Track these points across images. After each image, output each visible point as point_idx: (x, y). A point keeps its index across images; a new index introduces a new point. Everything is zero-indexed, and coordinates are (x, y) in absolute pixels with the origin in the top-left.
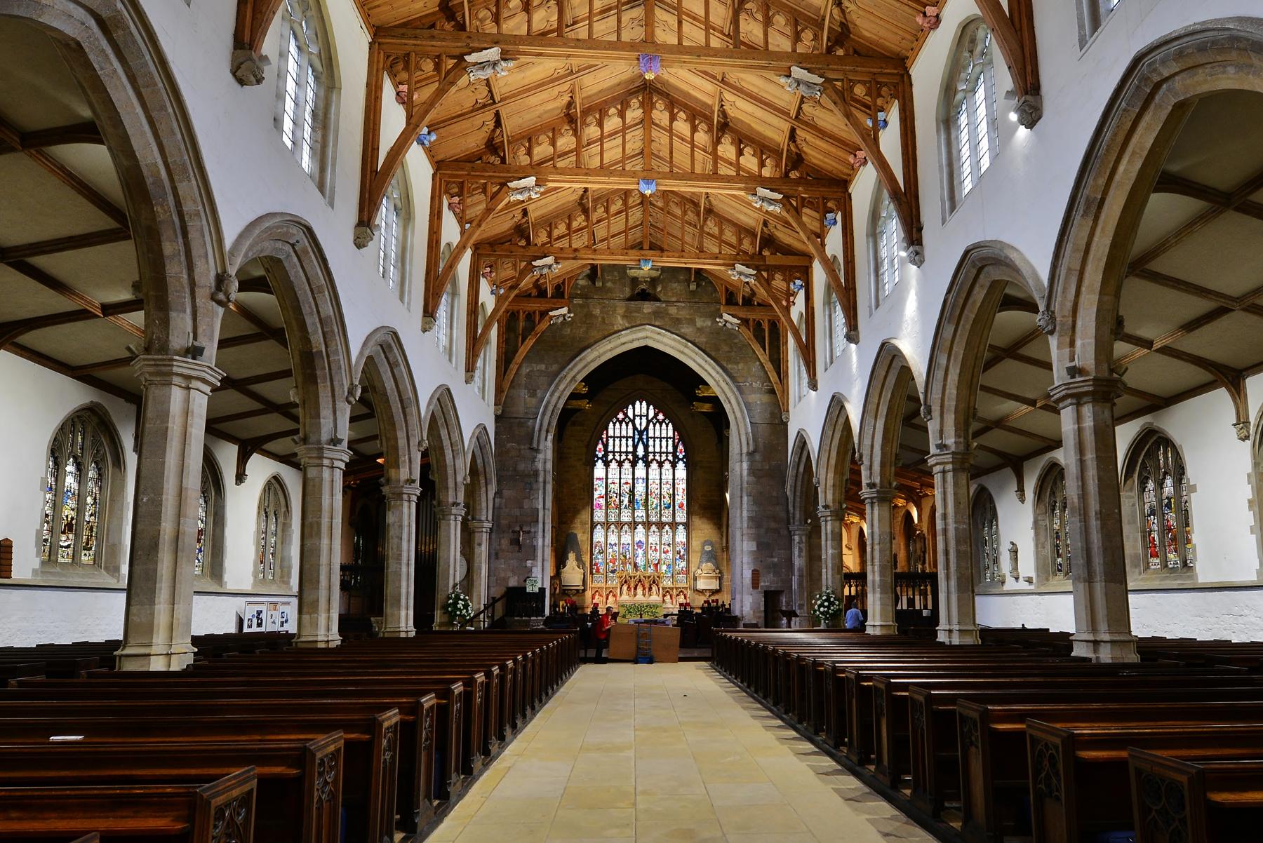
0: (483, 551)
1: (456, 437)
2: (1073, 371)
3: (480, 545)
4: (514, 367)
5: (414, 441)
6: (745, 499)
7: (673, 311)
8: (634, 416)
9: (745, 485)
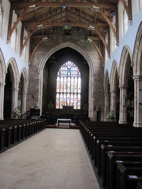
0: (25, 99)
1: (16, 70)
3: (24, 97)
4: (33, 52)
5: (4, 71)
6: (92, 87)
7: (75, 38)
8: (68, 65)
9: (93, 83)
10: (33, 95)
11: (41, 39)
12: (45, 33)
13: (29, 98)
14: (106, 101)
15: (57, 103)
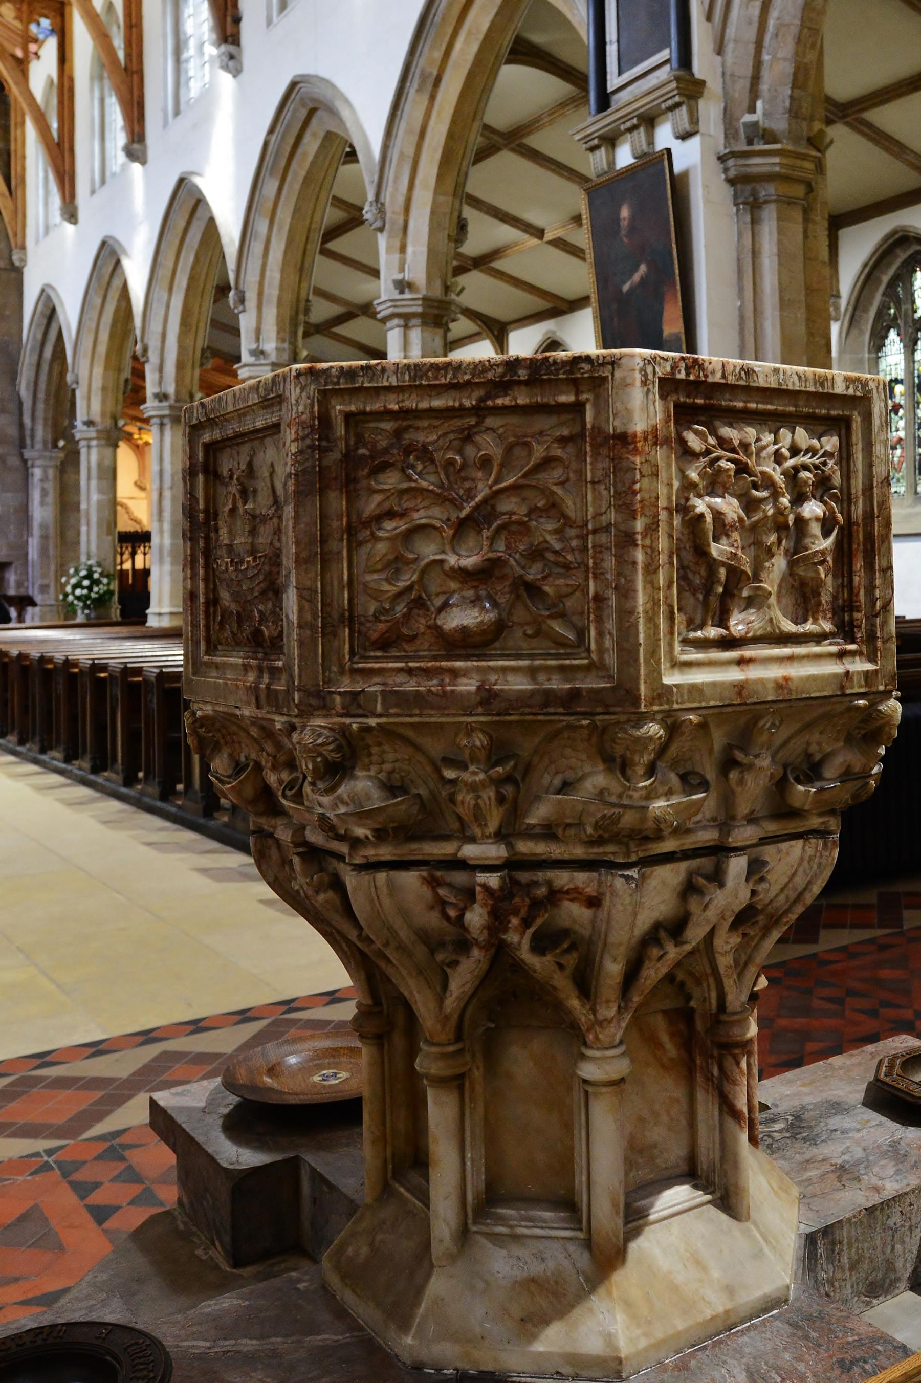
2: (402, 286)
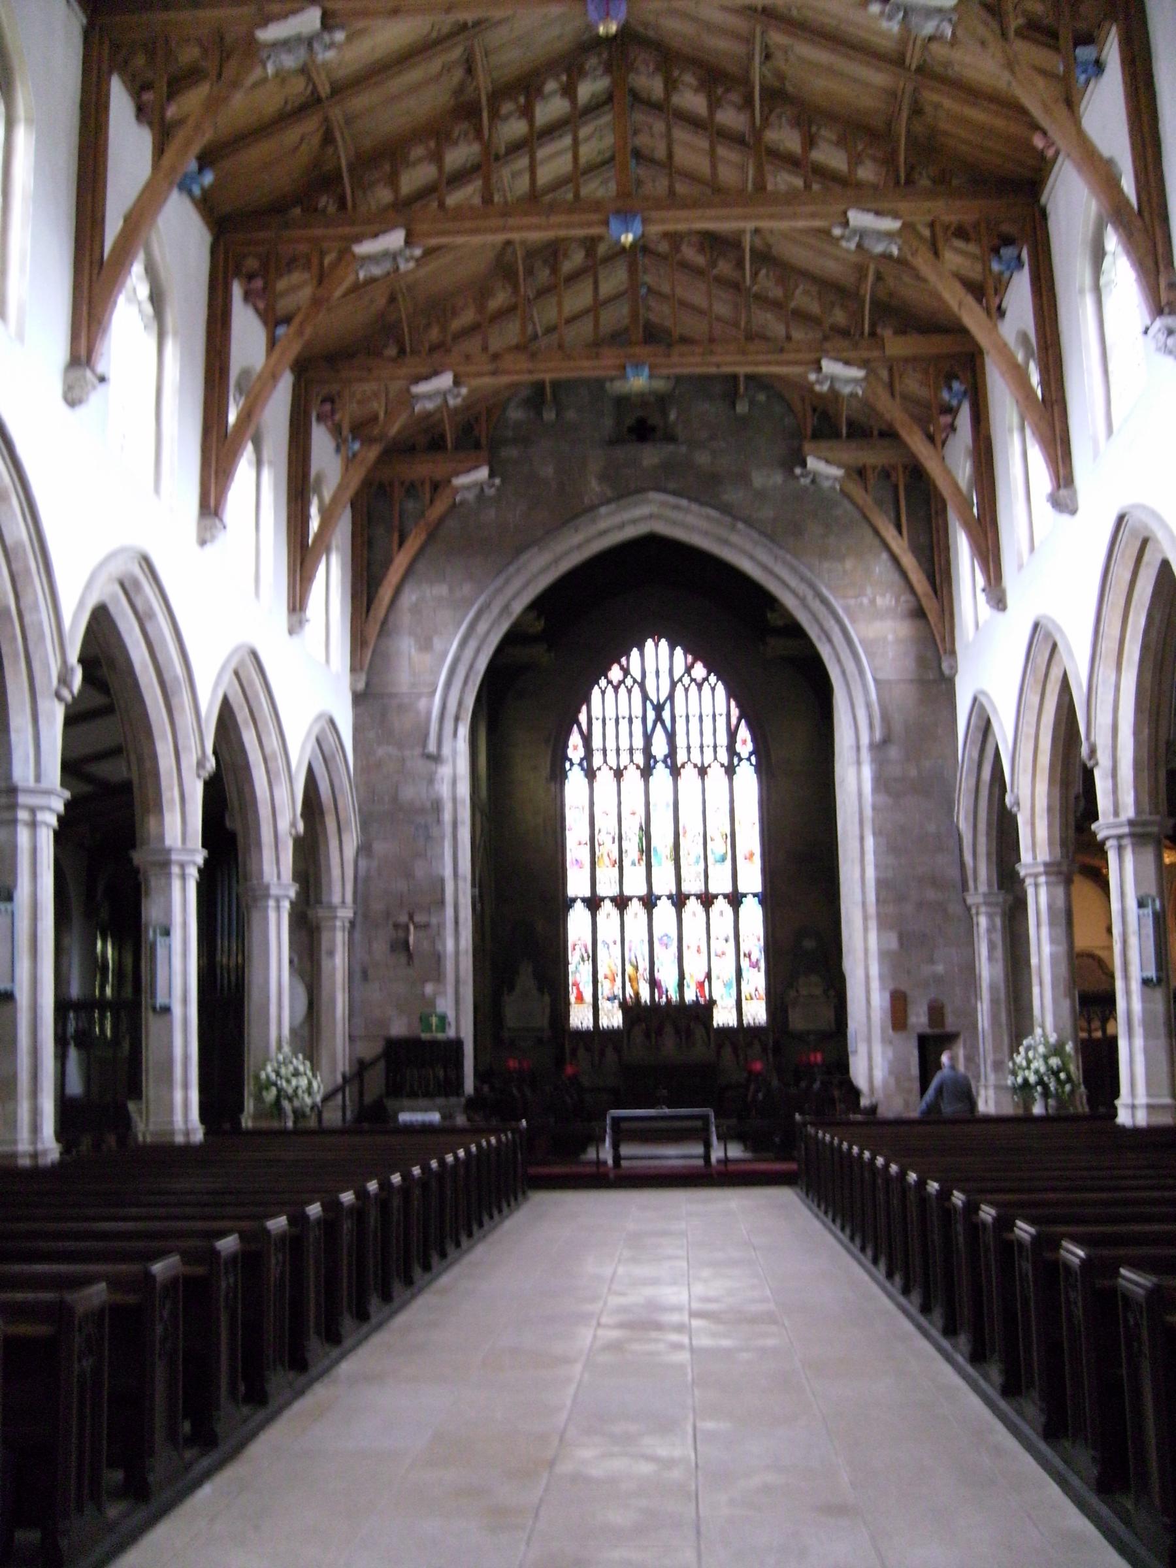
1: (272, 743)
3: (331, 953)
4: (385, 593)
5: (190, 760)
7: (702, 458)
9: (868, 812)
10: (398, 930)
11: (436, 487)
12: (469, 433)
13: (370, 952)
14: (983, 950)
15: (576, 984)
